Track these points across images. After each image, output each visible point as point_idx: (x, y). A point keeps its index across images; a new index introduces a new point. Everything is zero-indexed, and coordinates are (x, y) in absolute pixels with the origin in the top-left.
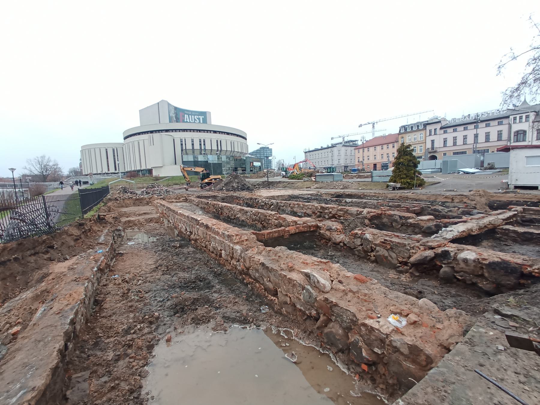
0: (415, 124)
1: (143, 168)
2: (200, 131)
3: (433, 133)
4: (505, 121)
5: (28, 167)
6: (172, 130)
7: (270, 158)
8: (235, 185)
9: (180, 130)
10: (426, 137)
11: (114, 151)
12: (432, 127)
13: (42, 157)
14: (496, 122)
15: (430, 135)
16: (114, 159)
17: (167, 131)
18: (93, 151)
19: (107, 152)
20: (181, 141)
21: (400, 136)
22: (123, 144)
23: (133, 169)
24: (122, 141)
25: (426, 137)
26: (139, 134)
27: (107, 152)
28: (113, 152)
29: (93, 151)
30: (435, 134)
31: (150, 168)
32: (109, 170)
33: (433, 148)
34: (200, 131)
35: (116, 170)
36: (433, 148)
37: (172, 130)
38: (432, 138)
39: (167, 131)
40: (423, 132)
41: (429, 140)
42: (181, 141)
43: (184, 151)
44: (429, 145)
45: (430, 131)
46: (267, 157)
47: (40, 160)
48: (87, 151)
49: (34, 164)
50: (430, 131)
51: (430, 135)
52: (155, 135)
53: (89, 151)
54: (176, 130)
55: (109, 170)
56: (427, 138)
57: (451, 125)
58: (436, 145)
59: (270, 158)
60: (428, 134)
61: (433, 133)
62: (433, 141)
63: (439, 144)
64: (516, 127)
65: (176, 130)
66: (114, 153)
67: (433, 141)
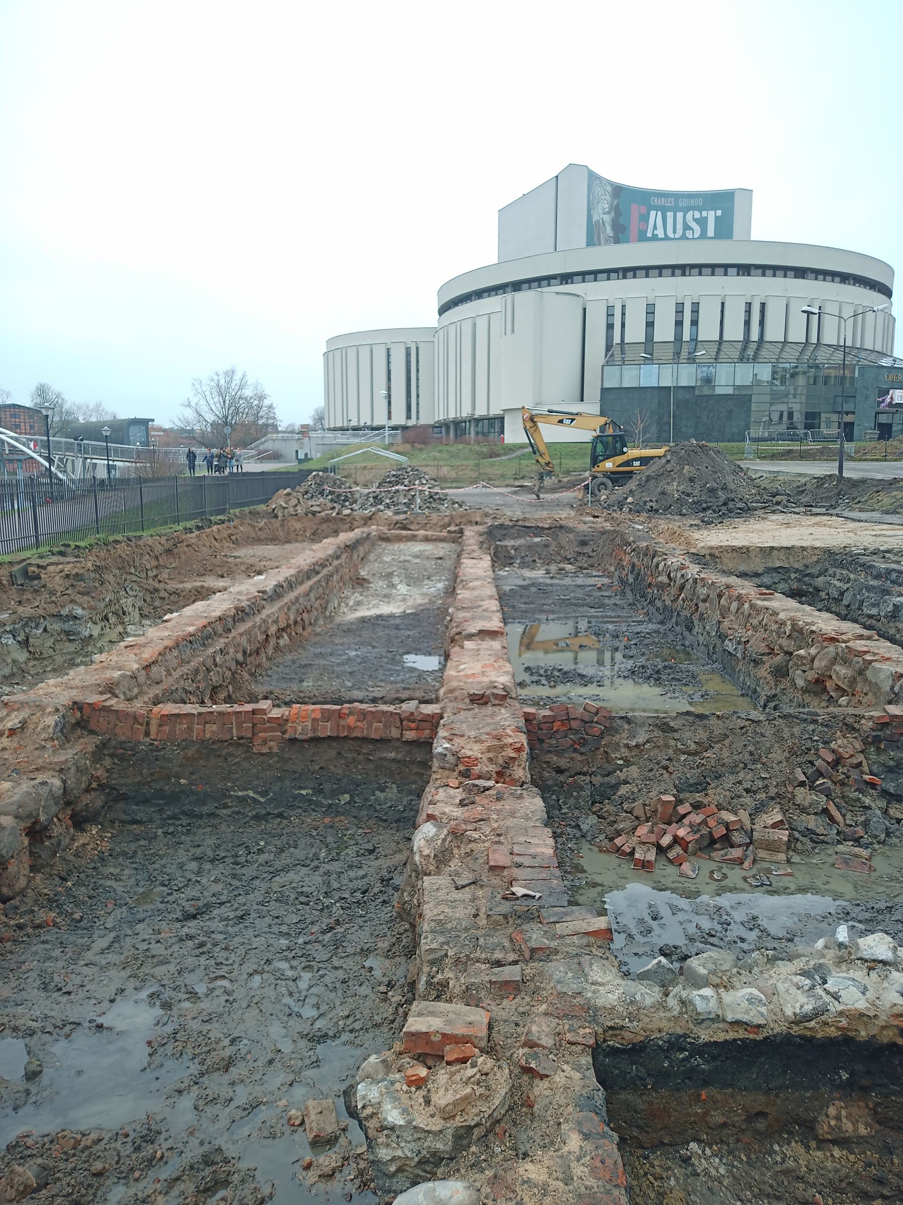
1: (481, 412)
2: (683, 269)
5: (194, 401)
6: (584, 275)
8: (674, 488)
9: (609, 273)
11: (408, 355)
13: (226, 373)
17: (566, 278)
18: (352, 354)
19: (389, 355)
20: (610, 315)
22: (436, 331)
24: (431, 319)
26: (479, 294)
27: (389, 355)
28: (407, 358)
29: (352, 354)
31: (495, 411)
32: (390, 418)
34: (683, 269)
35: (409, 417)
37: (584, 275)
39: (566, 278)
42: (610, 315)
43: (616, 350)
48: (338, 353)
49: (208, 394)
52: (524, 297)
53: (344, 351)
54: (595, 274)
55: (390, 418)
65: (595, 274)
66: (408, 363)
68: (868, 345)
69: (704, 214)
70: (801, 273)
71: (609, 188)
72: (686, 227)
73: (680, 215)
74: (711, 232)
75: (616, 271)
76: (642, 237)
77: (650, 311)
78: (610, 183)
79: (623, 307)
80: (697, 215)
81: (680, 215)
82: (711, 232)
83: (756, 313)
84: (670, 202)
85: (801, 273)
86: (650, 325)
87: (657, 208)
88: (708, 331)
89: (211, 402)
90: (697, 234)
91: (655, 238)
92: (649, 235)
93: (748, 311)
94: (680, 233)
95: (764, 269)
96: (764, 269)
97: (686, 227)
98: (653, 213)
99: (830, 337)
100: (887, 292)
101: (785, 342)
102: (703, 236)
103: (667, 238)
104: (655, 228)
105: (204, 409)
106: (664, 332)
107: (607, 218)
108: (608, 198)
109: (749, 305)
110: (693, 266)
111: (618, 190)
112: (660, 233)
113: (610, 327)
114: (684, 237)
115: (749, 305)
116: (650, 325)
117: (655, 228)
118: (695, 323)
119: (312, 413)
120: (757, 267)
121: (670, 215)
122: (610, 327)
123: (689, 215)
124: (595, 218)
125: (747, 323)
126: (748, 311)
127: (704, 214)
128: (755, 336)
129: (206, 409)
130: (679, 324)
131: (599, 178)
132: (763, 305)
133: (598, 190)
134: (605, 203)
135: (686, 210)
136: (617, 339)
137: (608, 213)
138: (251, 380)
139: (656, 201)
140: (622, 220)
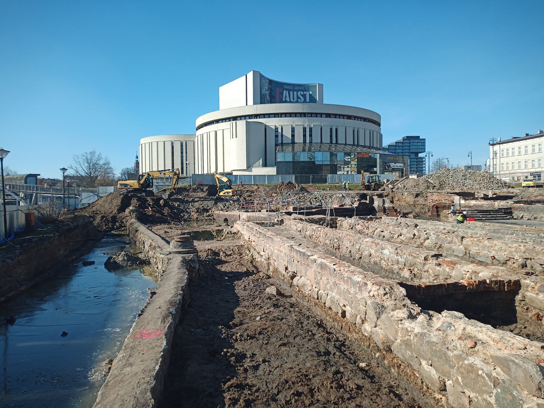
7: (420, 155)
16: (182, 157)
23: (206, 172)
46: (417, 154)
47: (89, 157)
59: (420, 155)
68: (375, 146)
69: (305, 93)
70: (349, 117)
71: (267, 81)
72: (298, 98)
73: (295, 93)
74: (308, 100)
75: (278, 114)
76: (281, 102)
77: (293, 130)
78: (268, 79)
79: (282, 128)
80: (302, 93)
81: (295, 93)
82: (308, 100)
83: (334, 133)
84: (291, 88)
85: (349, 117)
86: (293, 136)
87: (286, 90)
88: (316, 139)
89: (83, 166)
90: (302, 101)
91: (286, 102)
92: (284, 100)
93: (331, 132)
94: (295, 100)
95: (336, 116)
96: (336, 116)
97: (298, 98)
98: (285, 91)
99: (361, 143)
100: (379, 125)
101: (346, 144)
102: (305, 101)
103: (290, 102)
104: (286, 97)
105: (80, 169)
106: (299, 139)
107: (267, 93)
108: (267, 84)
109: (331, 129)
110: (308, 113)
111: (271, 82)
112: (288, 100)
113: (277, 136)
114: (297, 102)
115: (331, 129)
116: (293, 136)
117: (286, 97)
118: (311, 135)
119: (121, 171)
120: (333, 114)
121: (291, 92)
122: (277, 136)
123: (299, 93)
124: (263, 92)
125: (331, 136)
126: (331, 132)
127: (305, 93)
128: (334, 141)
129: (81, 169)
130: (305, 136)
131: (264, 77)
132: (336, 129)
133: (263, 81)
134: (266, 87)
135: (298, 91)
136: (280, 142)
137: (268, 91)
138: (103, 156)
139: (286, 87)
140: (273, 94)
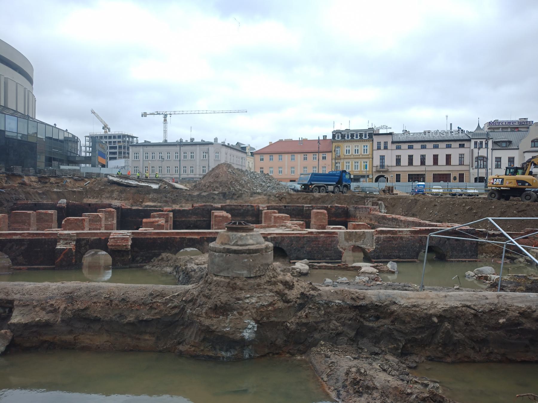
0: (365, 131)
3: (382, 147)
4: (466, 144)
10: (373, 150)
12: (382, 140)
14: (457, 144)
15: (379, 148)
21: (334, 144)
25: (373, 150)
30: (386, 148)
33: (382, 166)
36: (382, 166)
38: (382, 152)
40: (369, 144)
41: (377, 155)
44: (377, 162)
45: (379, 143)
50: (379, 143)
51: (379, 148)
56: (374, 151)
57: (418, 140)
58: (387, 163)
60: (375, 147)
61: (382, 147)
62: (382, 158)
63: (390, 161)
64: (483, 152)
67: (382, 158)
